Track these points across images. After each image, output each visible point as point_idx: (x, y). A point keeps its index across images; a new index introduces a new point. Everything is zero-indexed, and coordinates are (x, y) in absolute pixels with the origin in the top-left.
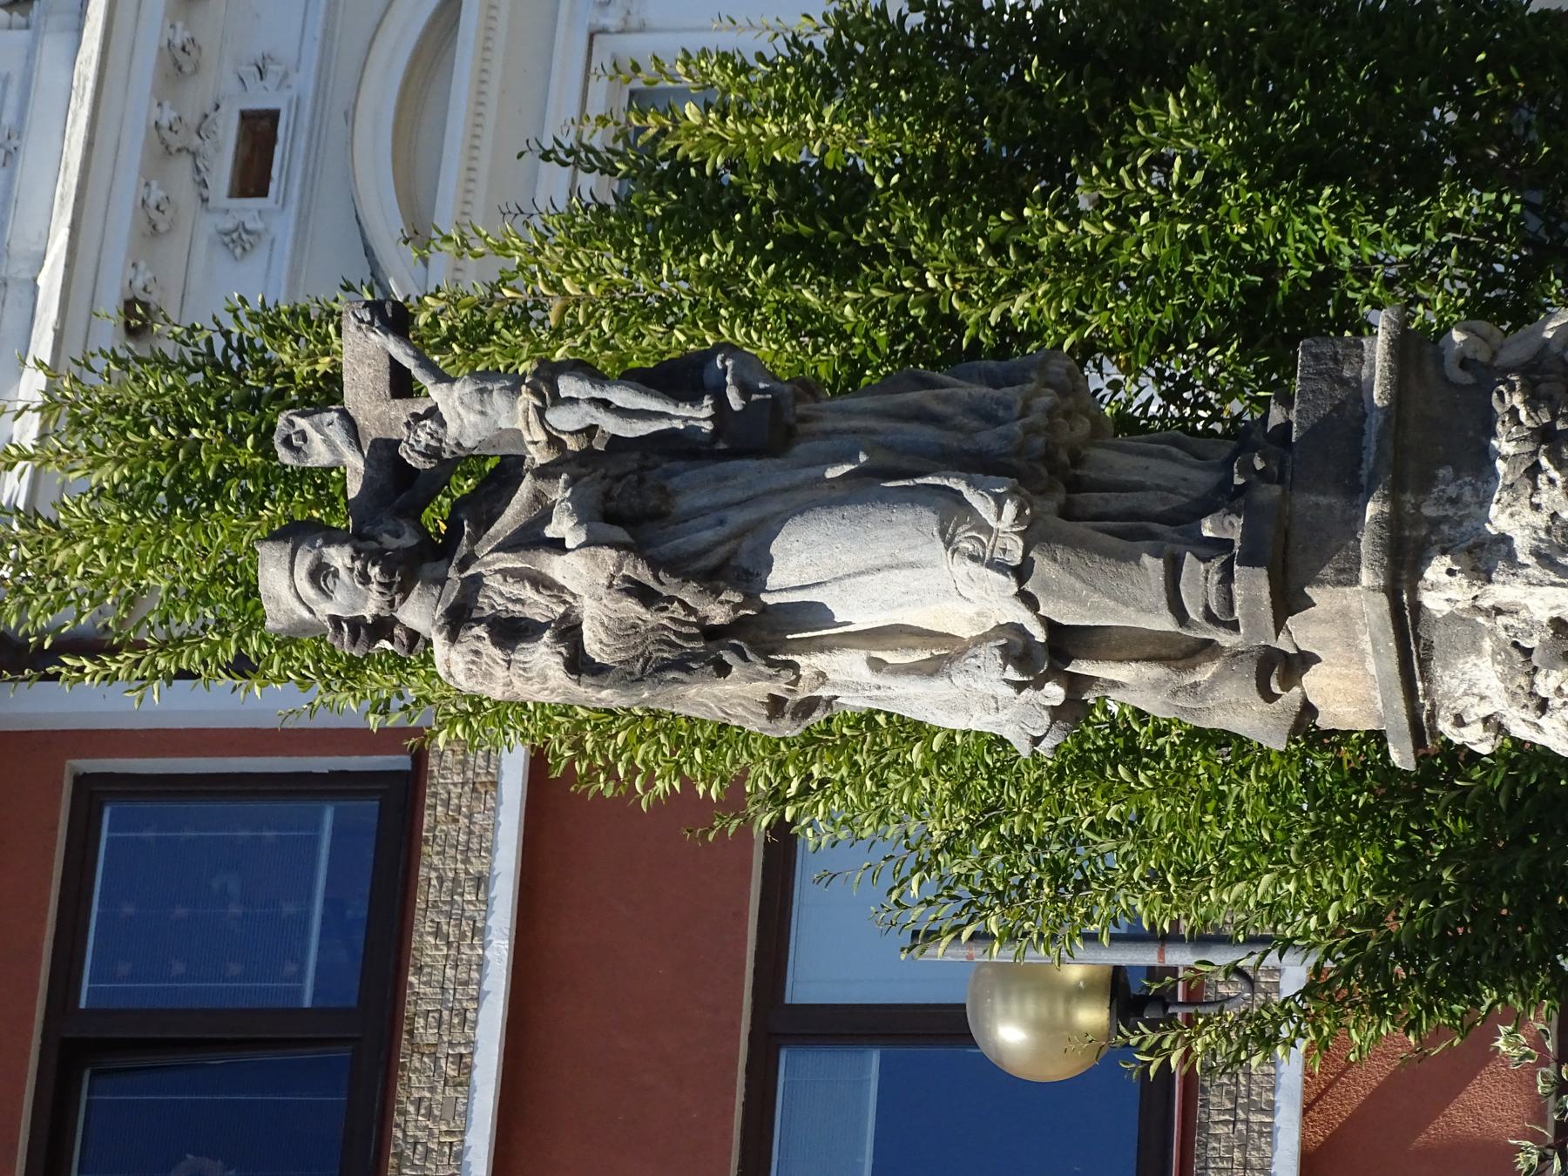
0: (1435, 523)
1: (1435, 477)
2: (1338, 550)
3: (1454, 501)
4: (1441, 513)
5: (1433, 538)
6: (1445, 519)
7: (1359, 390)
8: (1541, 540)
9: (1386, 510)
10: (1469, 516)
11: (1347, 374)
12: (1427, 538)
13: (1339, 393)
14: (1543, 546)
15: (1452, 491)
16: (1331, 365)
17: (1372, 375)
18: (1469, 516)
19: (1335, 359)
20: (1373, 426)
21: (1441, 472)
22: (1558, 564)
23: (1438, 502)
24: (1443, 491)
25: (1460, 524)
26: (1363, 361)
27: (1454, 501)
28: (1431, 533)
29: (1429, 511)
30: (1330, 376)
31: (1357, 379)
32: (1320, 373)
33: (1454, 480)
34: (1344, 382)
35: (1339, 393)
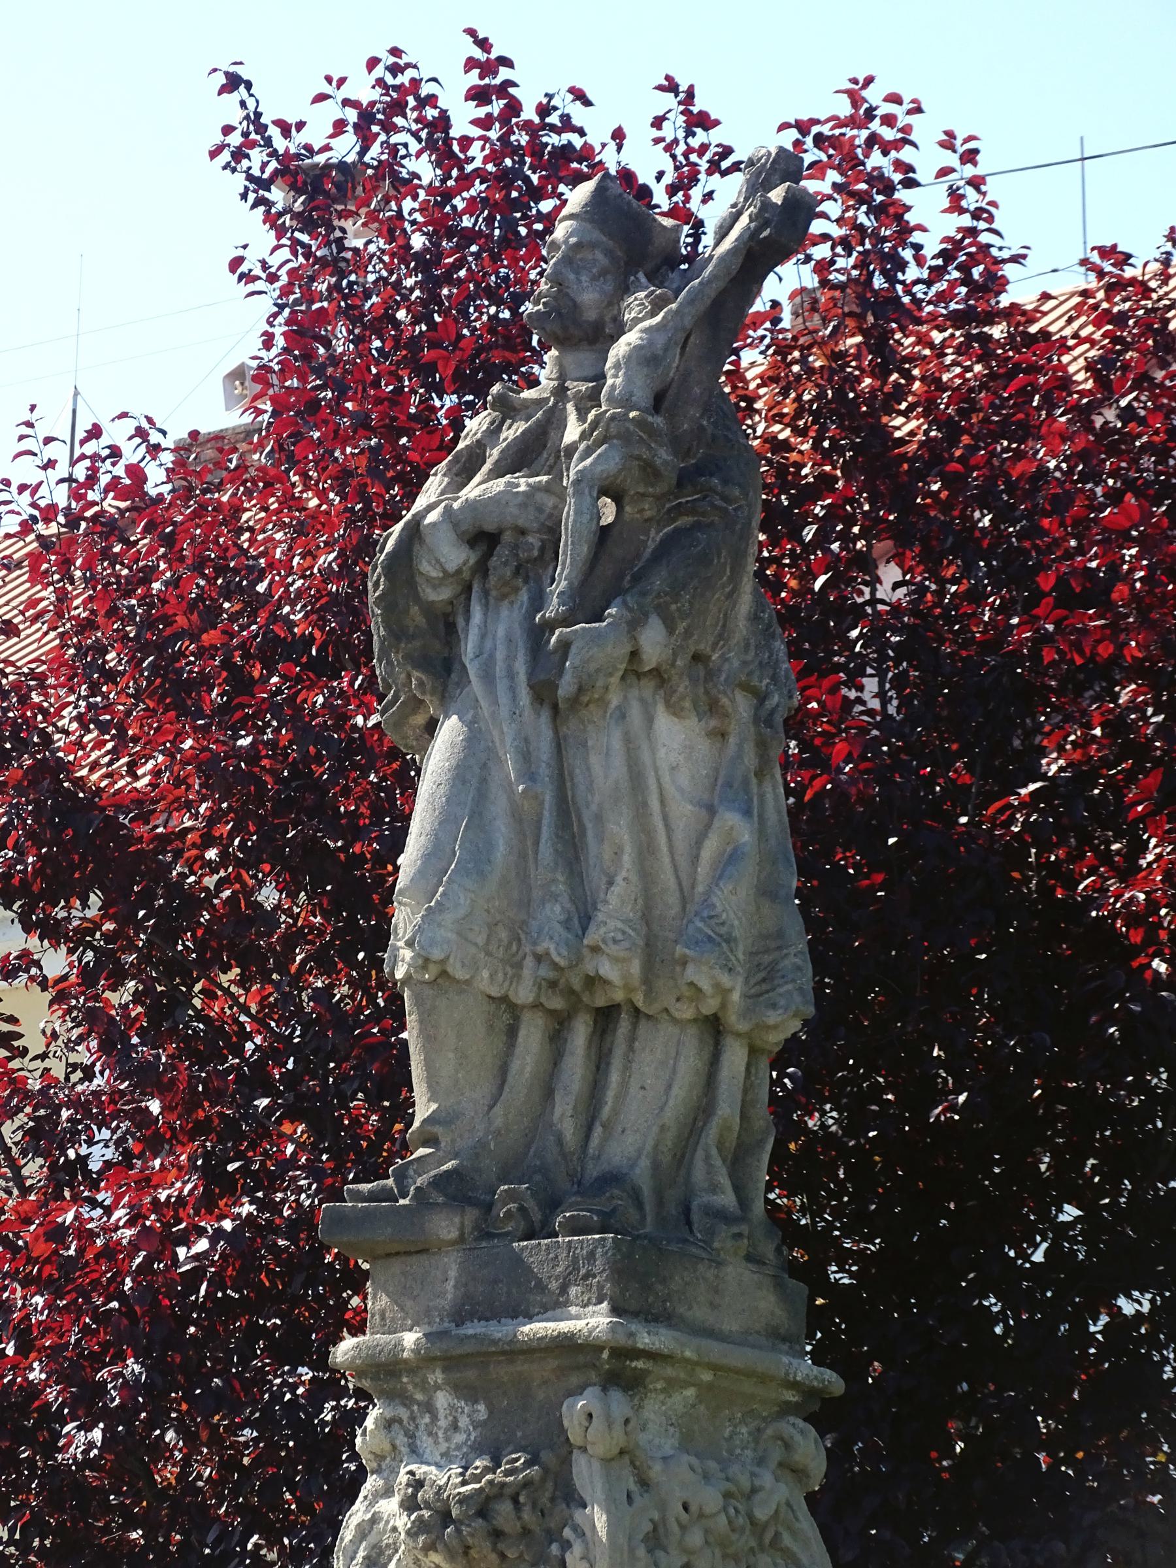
0: (429, 1408)
1: (476, 1402)
2: (402, 1309)
3: (455, 1427)
4: (441, 1413)
5: (415, 1407)
6: (435, 1418)
7: (557, 1305)
8: (387, 1522)
9: (405, 1355)
10: (436, 1443)
11: (573, 1291)
12: (414, 1401)
13: (554, 1285)
14: (381, 1525)
15: (464, 1422)
16: (583, 1272)
17: (570, 1318)
18: (436, 1443)
19: (586, 1277)
20: (498, 1330)
21: (481, 1407)
22: (361, 1542)
23: (452, 1407)
24: (463, 1412)
25: (430, 1434)
26: (585, 1306)
27: (455, 1427)
28: (419, 1404)
29: (442, 1400)
30: (570, 1273)
31: (567, 1304)
32: (575, 1260)
33: (472, 1422)
34: (564, 1289)
35: (554, 1285)
